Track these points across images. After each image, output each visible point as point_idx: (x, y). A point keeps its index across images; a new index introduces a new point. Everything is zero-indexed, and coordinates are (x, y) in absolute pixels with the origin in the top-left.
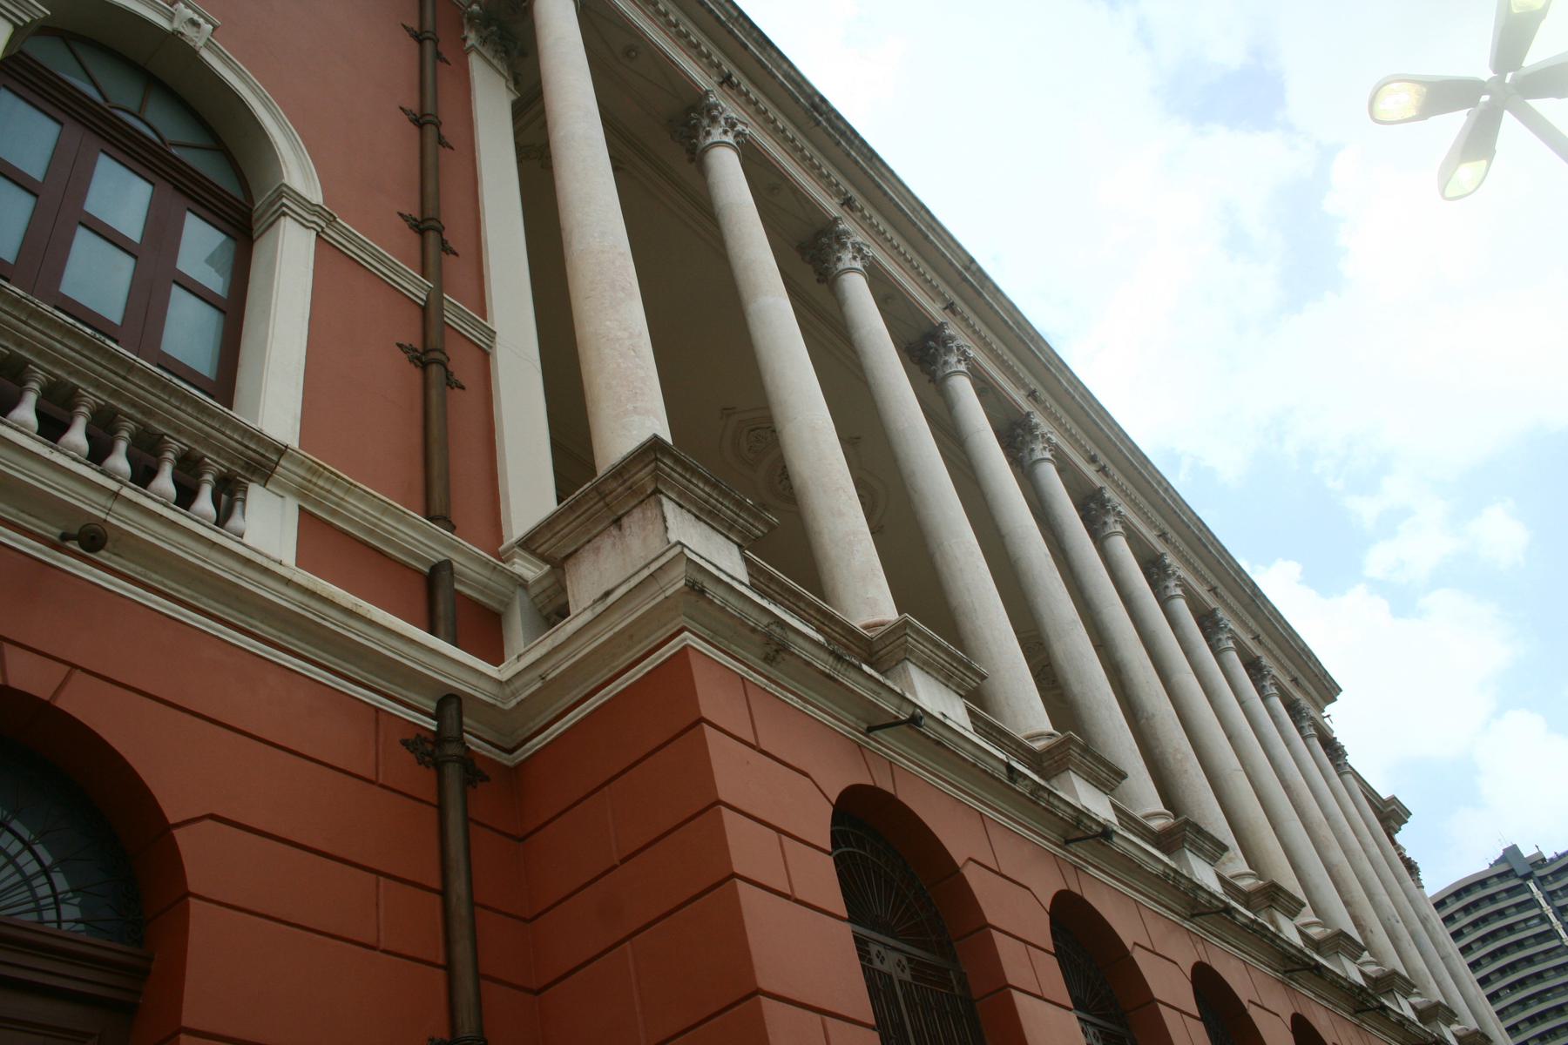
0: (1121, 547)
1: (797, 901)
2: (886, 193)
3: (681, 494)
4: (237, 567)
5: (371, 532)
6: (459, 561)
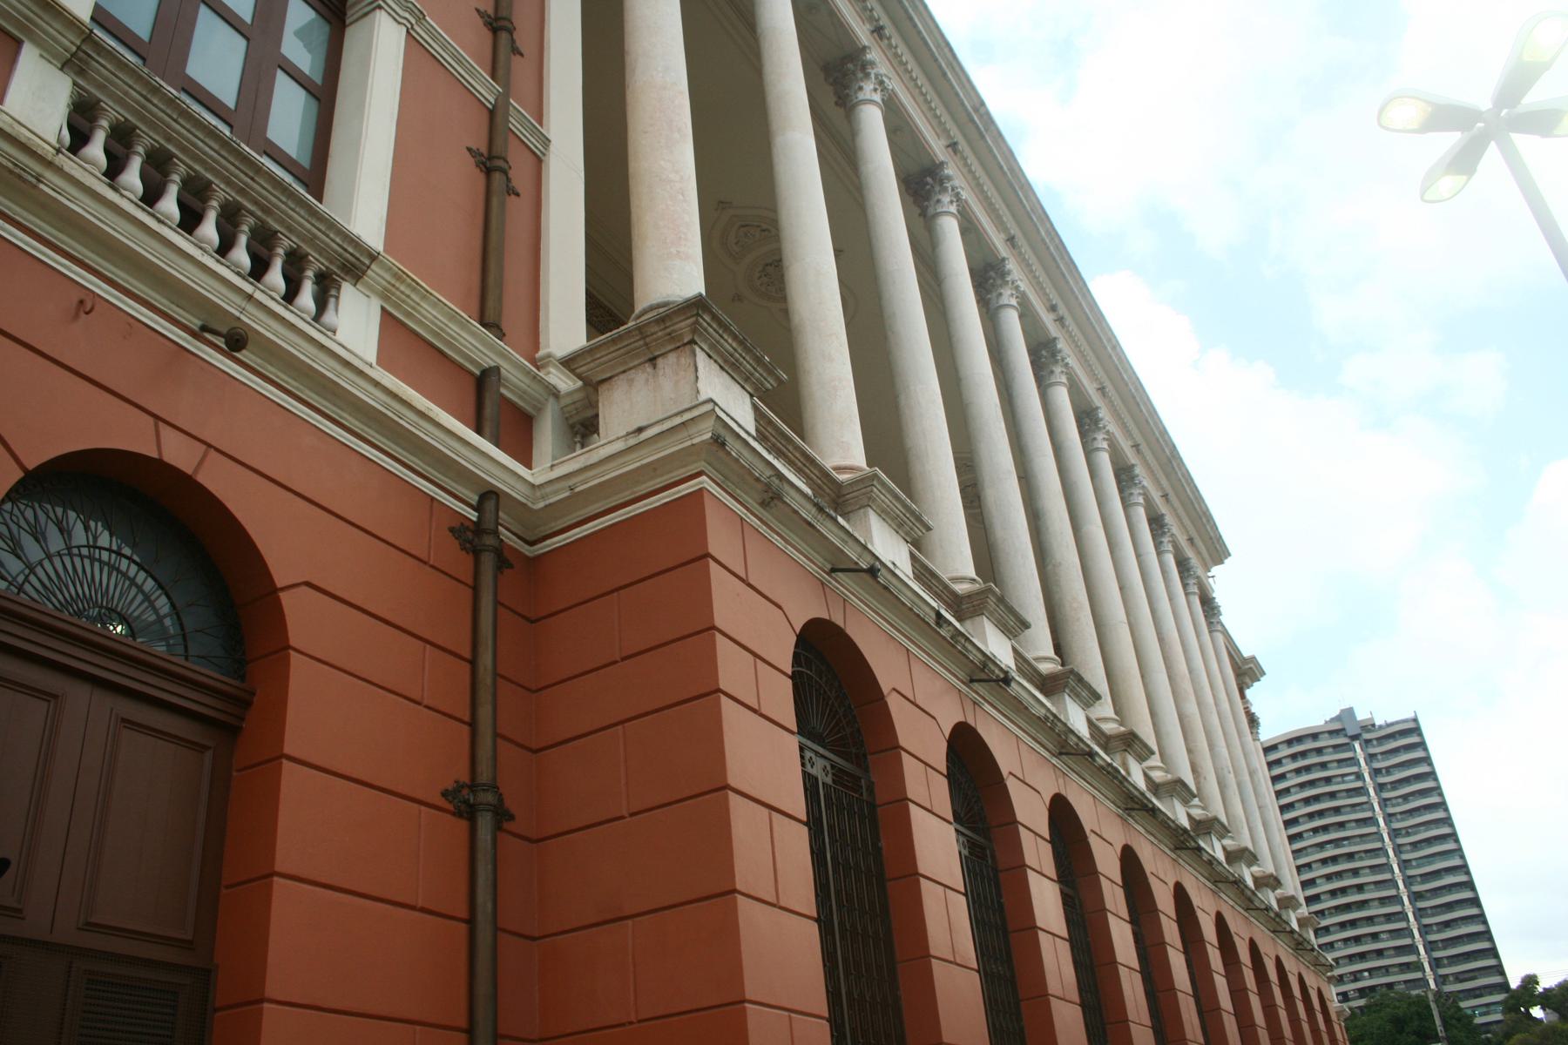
0: (1062, 397)
1: (762, 715)
2: (915, 26)
3: (712, 346)
4: (338, 367)
5: (437, 335)
6: (507, 370)
